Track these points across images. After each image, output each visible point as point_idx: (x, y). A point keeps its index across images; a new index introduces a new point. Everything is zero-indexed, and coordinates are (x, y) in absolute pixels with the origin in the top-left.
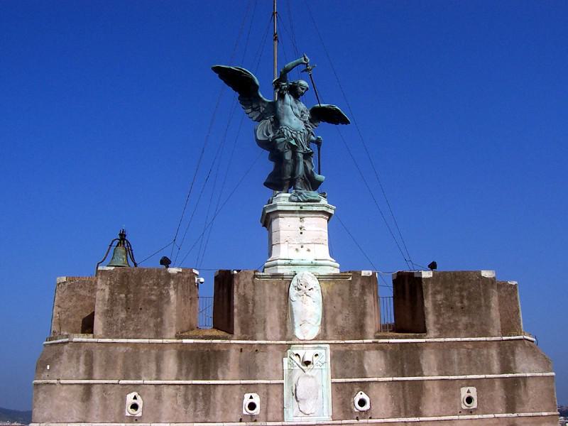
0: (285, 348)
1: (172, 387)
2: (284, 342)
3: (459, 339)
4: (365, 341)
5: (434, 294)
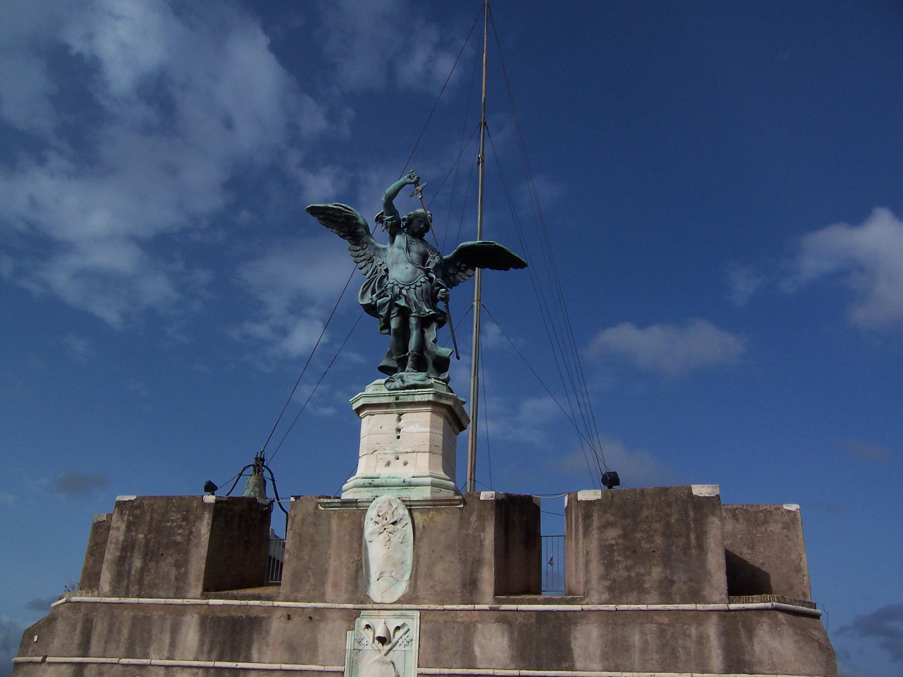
0: (352, 616)
1: (189, 670)
2: (351, 606)
3: (643, 607)
4: (477, 607)
5: (603, 527)
